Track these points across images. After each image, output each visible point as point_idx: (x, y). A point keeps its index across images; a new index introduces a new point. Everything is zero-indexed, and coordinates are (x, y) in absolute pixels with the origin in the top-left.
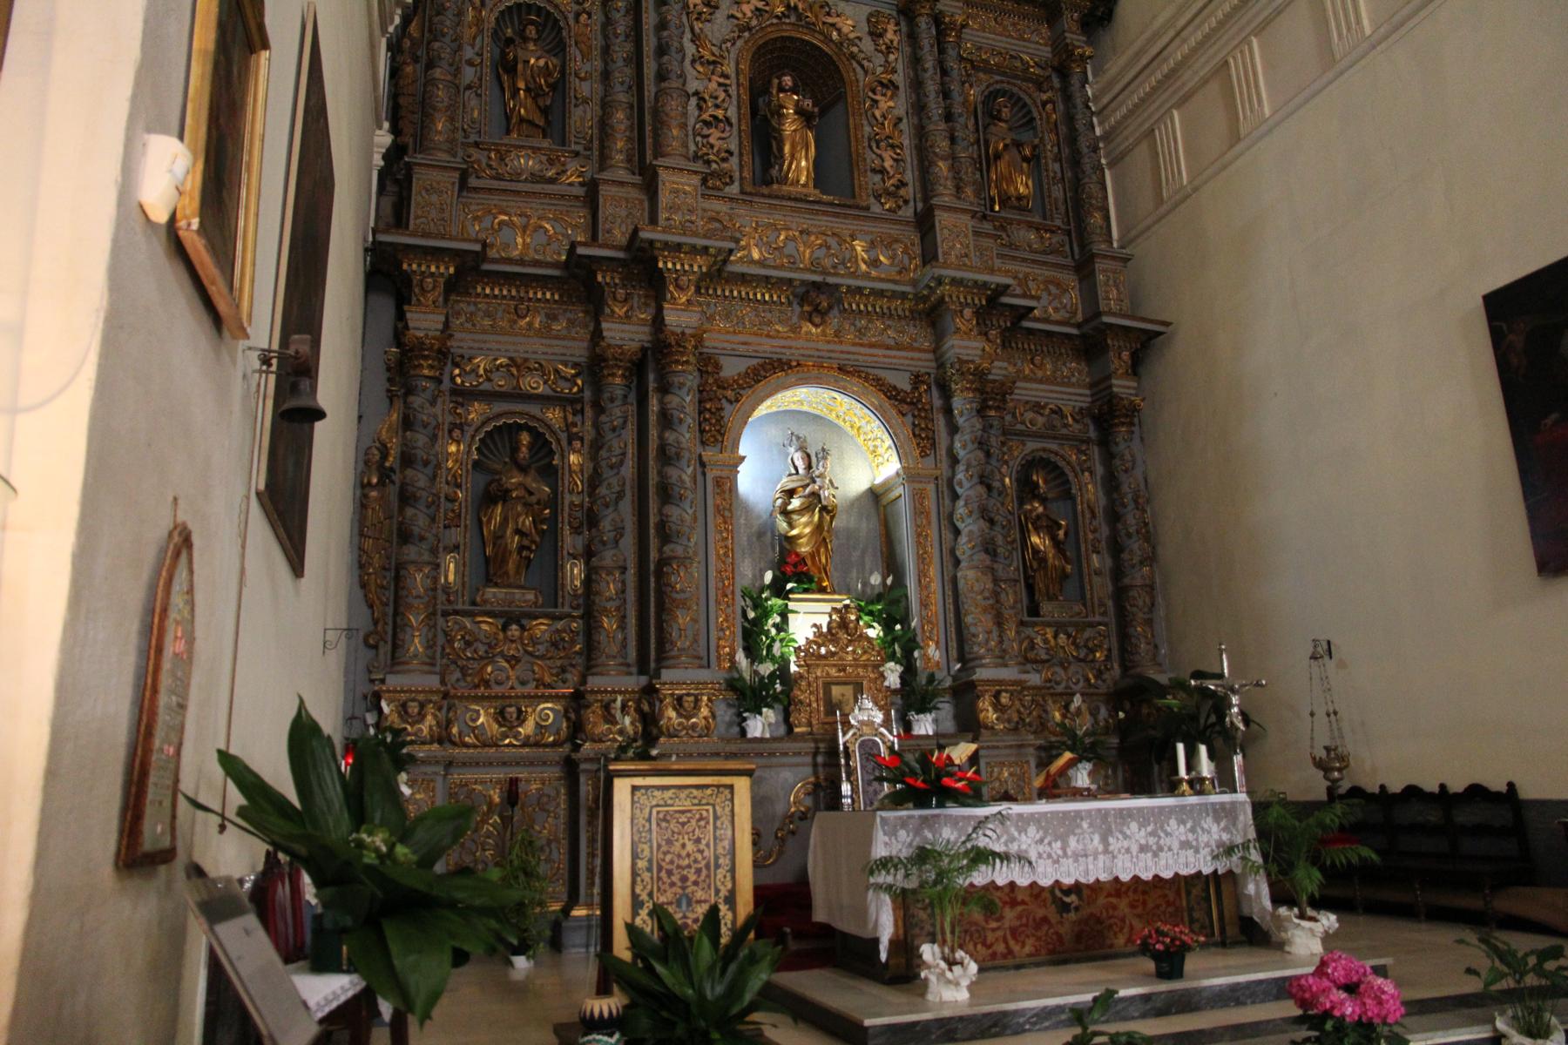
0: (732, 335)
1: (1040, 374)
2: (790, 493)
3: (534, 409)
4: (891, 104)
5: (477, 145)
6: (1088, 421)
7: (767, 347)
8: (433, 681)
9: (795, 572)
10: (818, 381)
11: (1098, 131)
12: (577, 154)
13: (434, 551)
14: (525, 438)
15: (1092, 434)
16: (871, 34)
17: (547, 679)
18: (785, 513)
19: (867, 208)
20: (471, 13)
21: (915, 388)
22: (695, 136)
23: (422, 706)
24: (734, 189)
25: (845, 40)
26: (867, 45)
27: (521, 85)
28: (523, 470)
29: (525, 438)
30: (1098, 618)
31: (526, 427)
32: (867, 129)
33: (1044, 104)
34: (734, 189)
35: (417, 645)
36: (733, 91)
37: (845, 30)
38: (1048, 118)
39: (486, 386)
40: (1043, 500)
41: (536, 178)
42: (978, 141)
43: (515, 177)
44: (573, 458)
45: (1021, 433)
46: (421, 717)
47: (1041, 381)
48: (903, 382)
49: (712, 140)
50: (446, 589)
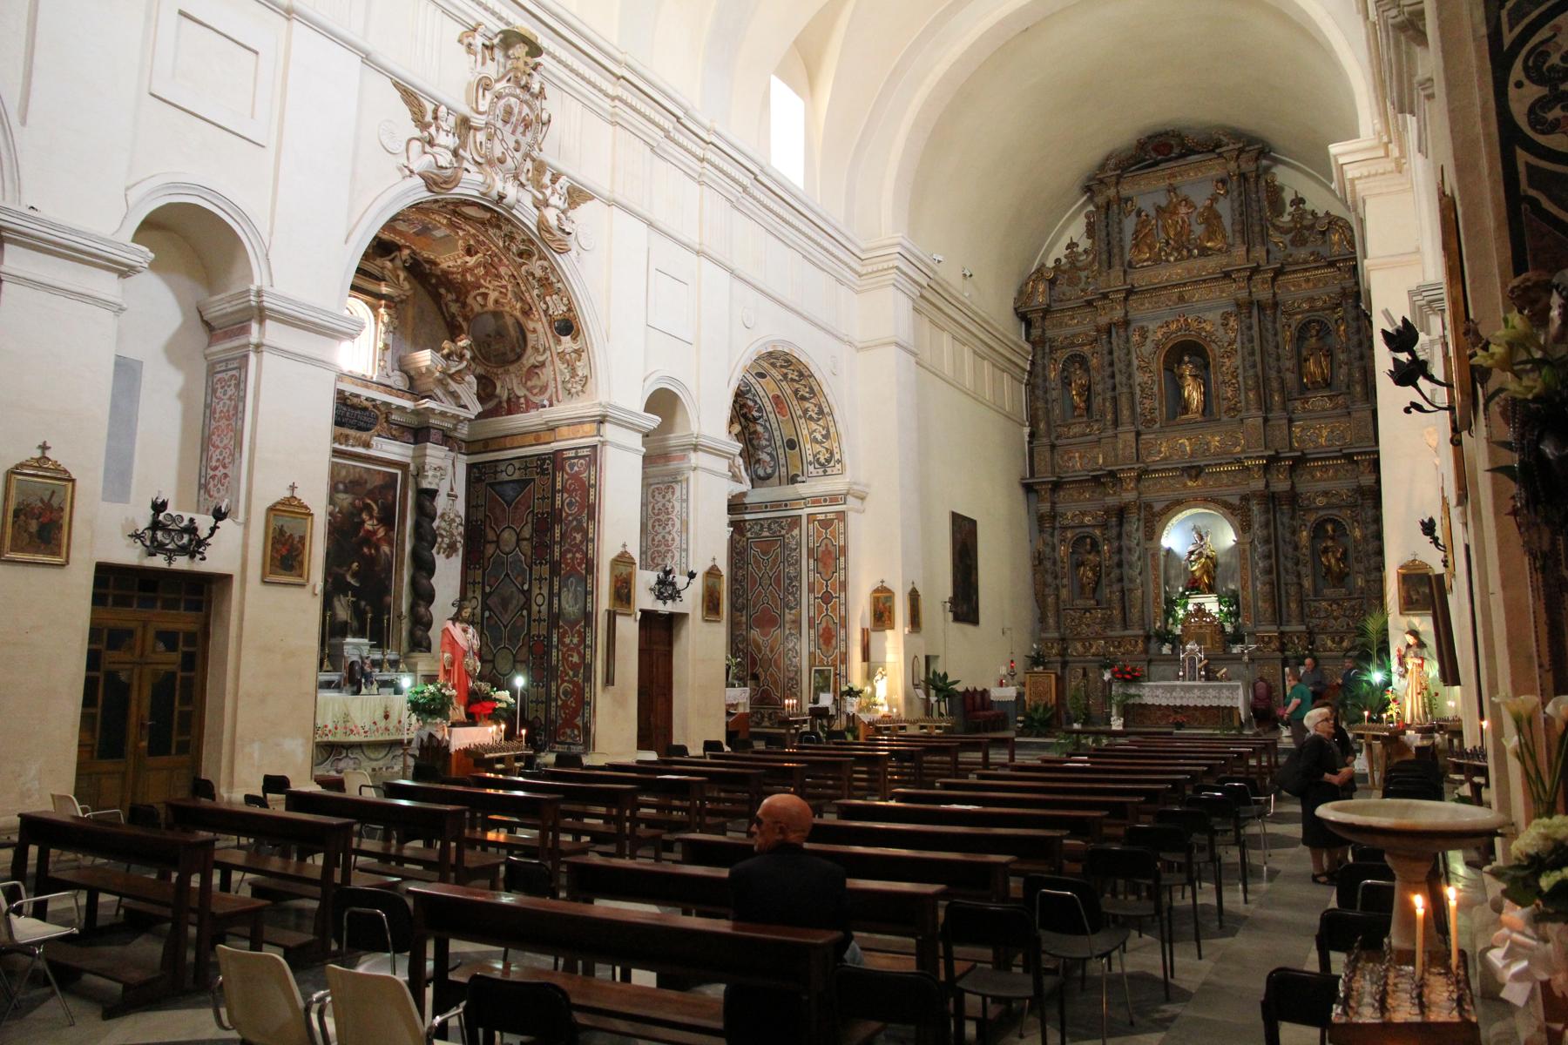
0: (1156, 494)
2: (1192, 553)
7: (1172, 495)
8: (1056, 635)
9: (1194, 586)
10: (1196, 506)
13: (1057, 588)
25: (1211, 334)
26: (1221, 330)
35: (1051, 621)
40: (1332, 538)
48: (1235, 501)
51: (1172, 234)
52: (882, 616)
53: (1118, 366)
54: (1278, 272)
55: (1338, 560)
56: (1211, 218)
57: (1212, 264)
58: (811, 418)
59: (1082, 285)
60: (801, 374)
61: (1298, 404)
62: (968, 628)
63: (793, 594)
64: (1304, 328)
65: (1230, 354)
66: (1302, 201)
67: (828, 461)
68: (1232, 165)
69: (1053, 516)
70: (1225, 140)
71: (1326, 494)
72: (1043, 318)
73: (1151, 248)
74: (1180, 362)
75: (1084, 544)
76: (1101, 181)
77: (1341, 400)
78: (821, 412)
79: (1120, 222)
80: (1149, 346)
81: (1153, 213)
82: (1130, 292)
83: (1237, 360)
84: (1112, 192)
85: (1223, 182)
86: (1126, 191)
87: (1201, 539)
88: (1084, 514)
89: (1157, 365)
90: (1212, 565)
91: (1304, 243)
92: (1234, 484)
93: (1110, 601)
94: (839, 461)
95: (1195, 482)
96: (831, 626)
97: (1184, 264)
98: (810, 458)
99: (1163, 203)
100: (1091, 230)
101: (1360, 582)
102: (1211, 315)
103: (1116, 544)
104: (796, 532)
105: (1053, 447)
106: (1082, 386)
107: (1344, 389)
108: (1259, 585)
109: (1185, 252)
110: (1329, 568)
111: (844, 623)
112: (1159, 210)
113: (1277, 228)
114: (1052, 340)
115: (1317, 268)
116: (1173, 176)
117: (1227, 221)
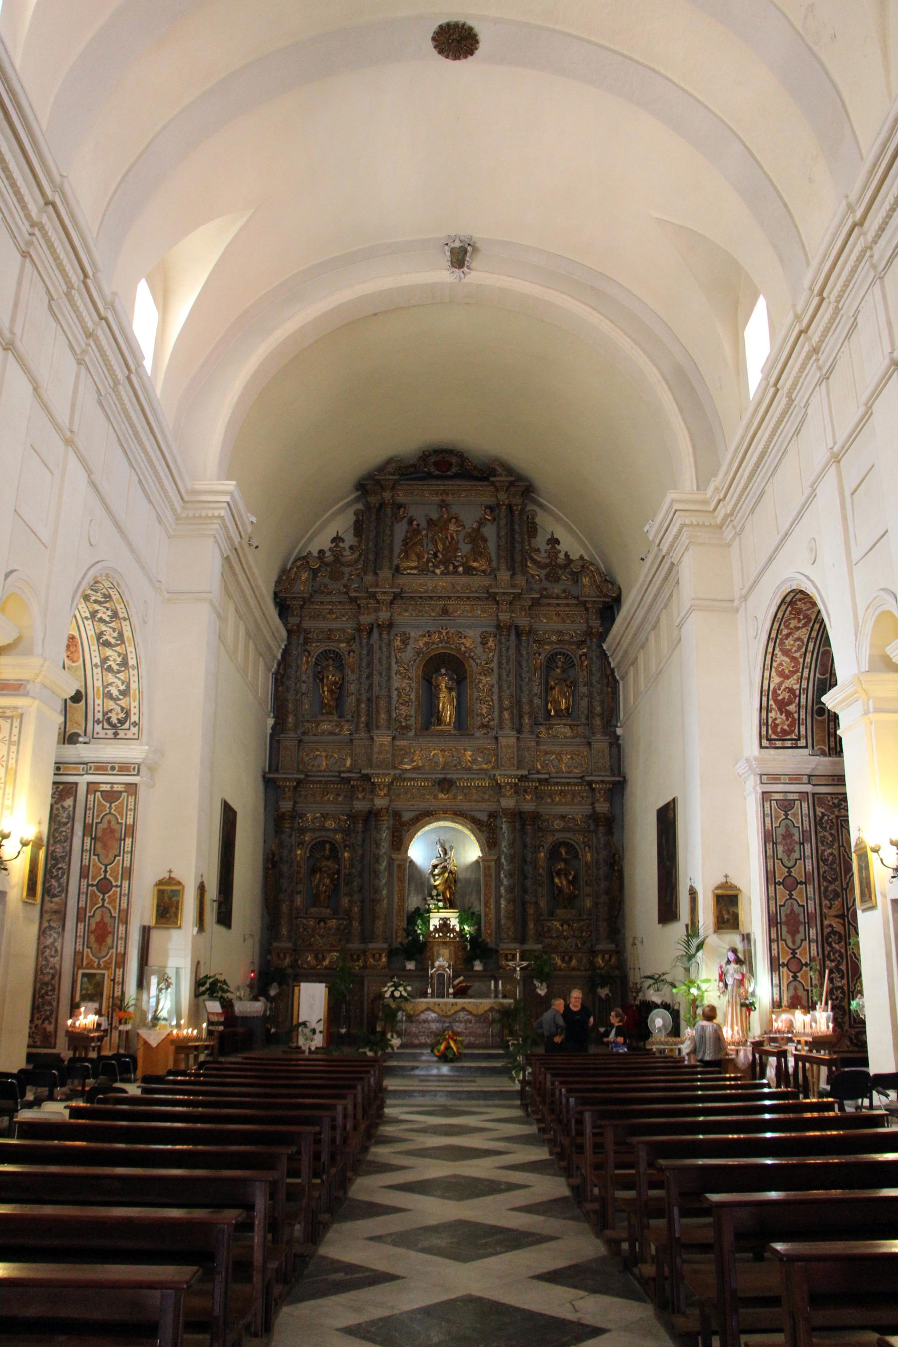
1: (564, 801)
2: (435, 866)
3: (331, 834)
4: (488, 679)
5: (308, 721)
6: (591, 821)
7: (423, 806)
8: (290, 945)
11: (612, 665)
12: (348, 721)
14: (328, 846)
15: (592, 828)
16: (482, 643)
17: (334, 943)
18: (434, 876)
19: (473, 735)
20: (305, 658)
21: (489, 819)
22: (396, 709)
23: (285, 955)
24: (412, 734)
26: (480, 649)
27: (326, 689)
28: (328, 859)
29: (328, 846)
30: (585, 917)
31: (327, 842)
32: (476, 694)
33: (581, 656)
34: (412, 734)
35: (284, 931)
36: (414, 685)
37: (468, 645)
38: (582, 662)
39: (312, 826)
41: (332, 734)
42: (541, 684)
43: (323, 734)
44: (346, 854)
45: (550, 831)
46: (285, 958)
47: (564, 805)
48: (484, 817)
49: (402, 712)
50: (297, 909)
51: (440, 547)
52: (167, 910)
53: (377, 665)
54: (536, 603)
55: (569, 882)
56: (476, 538)
57: (478, 582)
58: (110, 669)
59: (345, 581)
60: (115, 615)
61: (542, 729)
62: (222, 930)
63: (58, 878)
64: (551, 659)
65: (488, 672)
66: (557, 542)
67: (122, 722)
68: (502, 496)
69: (295, 815)
70: (499, 470)
71: (563, 817)
72: (302, 607)
73: (419, 557)
74: (437, 670)
75: (324, 850)
76: (378, 482)
77: (580, 730)
78: (124, 663)
79: (391, 526)
80: (409, 653)
81: (423, 524)
82: (396, 596)
83: (492, 680)
84: (387, 495)
85: (491, 509)
86: (401, 498)
87: (445, 853)
88: (325, 816)
89: (415, 672)
90: (452, 879)
91: (558, 580)
92: (483, 800)
93: (348, 913)
94: (135, 724)
95: (444, 796)
96: (107, 920)
97: (449, 578)
98: (99, 716)
99: (435, 516)
100: (358, 528)
101: (588, 904)
102: (471, 632)
103: (360, 852)
104: (69, 802)
105: (300, 741)
106: (335, 683)
107: (583, 720)
108: (503, 904)
109: (451, 568)
110: (561, 890)
111: (124, 917)
112: (430, 523)
113: (534, 561)
114: (307, 631)
115: (567, 605)
116: (445, 493)
117: (492, 545)
